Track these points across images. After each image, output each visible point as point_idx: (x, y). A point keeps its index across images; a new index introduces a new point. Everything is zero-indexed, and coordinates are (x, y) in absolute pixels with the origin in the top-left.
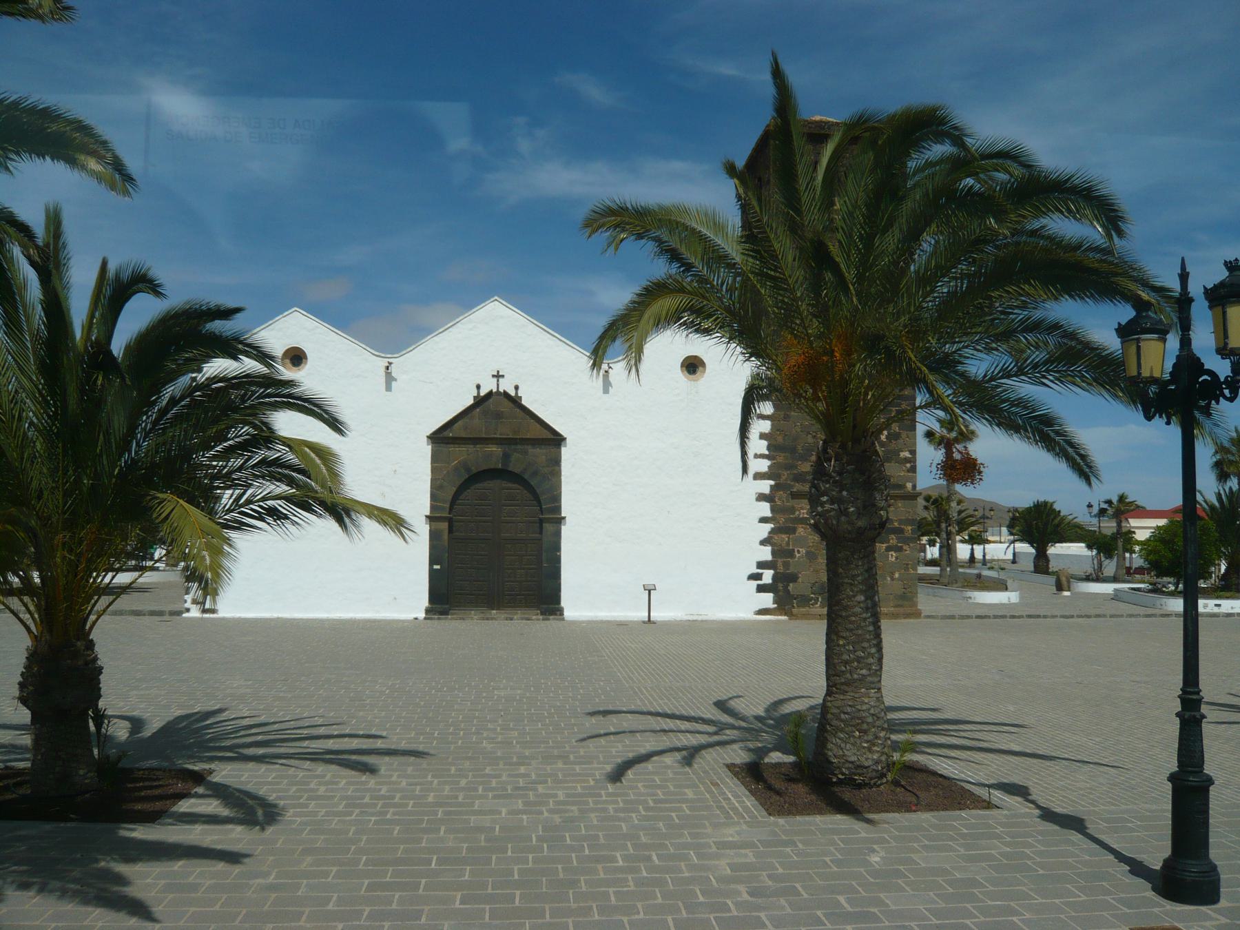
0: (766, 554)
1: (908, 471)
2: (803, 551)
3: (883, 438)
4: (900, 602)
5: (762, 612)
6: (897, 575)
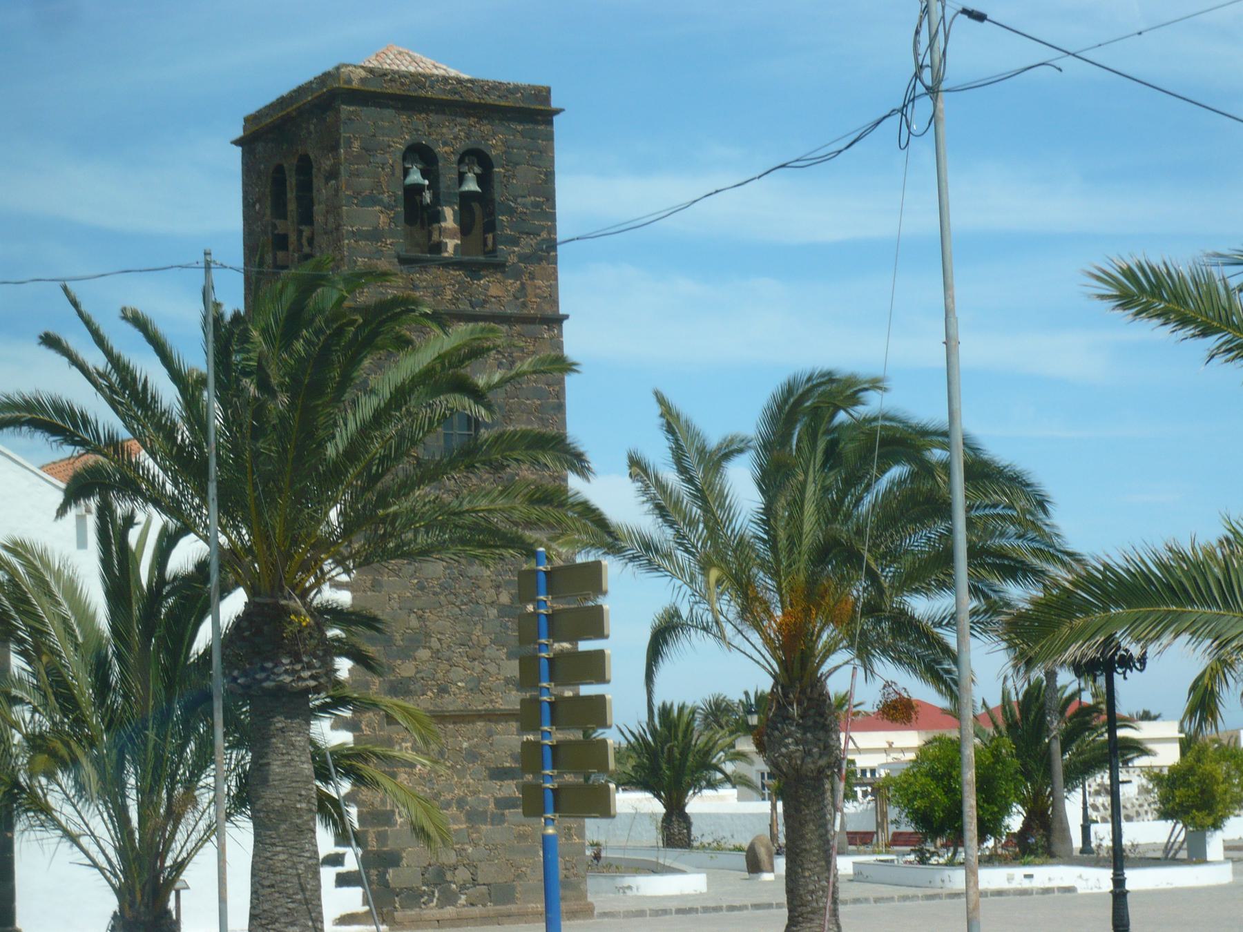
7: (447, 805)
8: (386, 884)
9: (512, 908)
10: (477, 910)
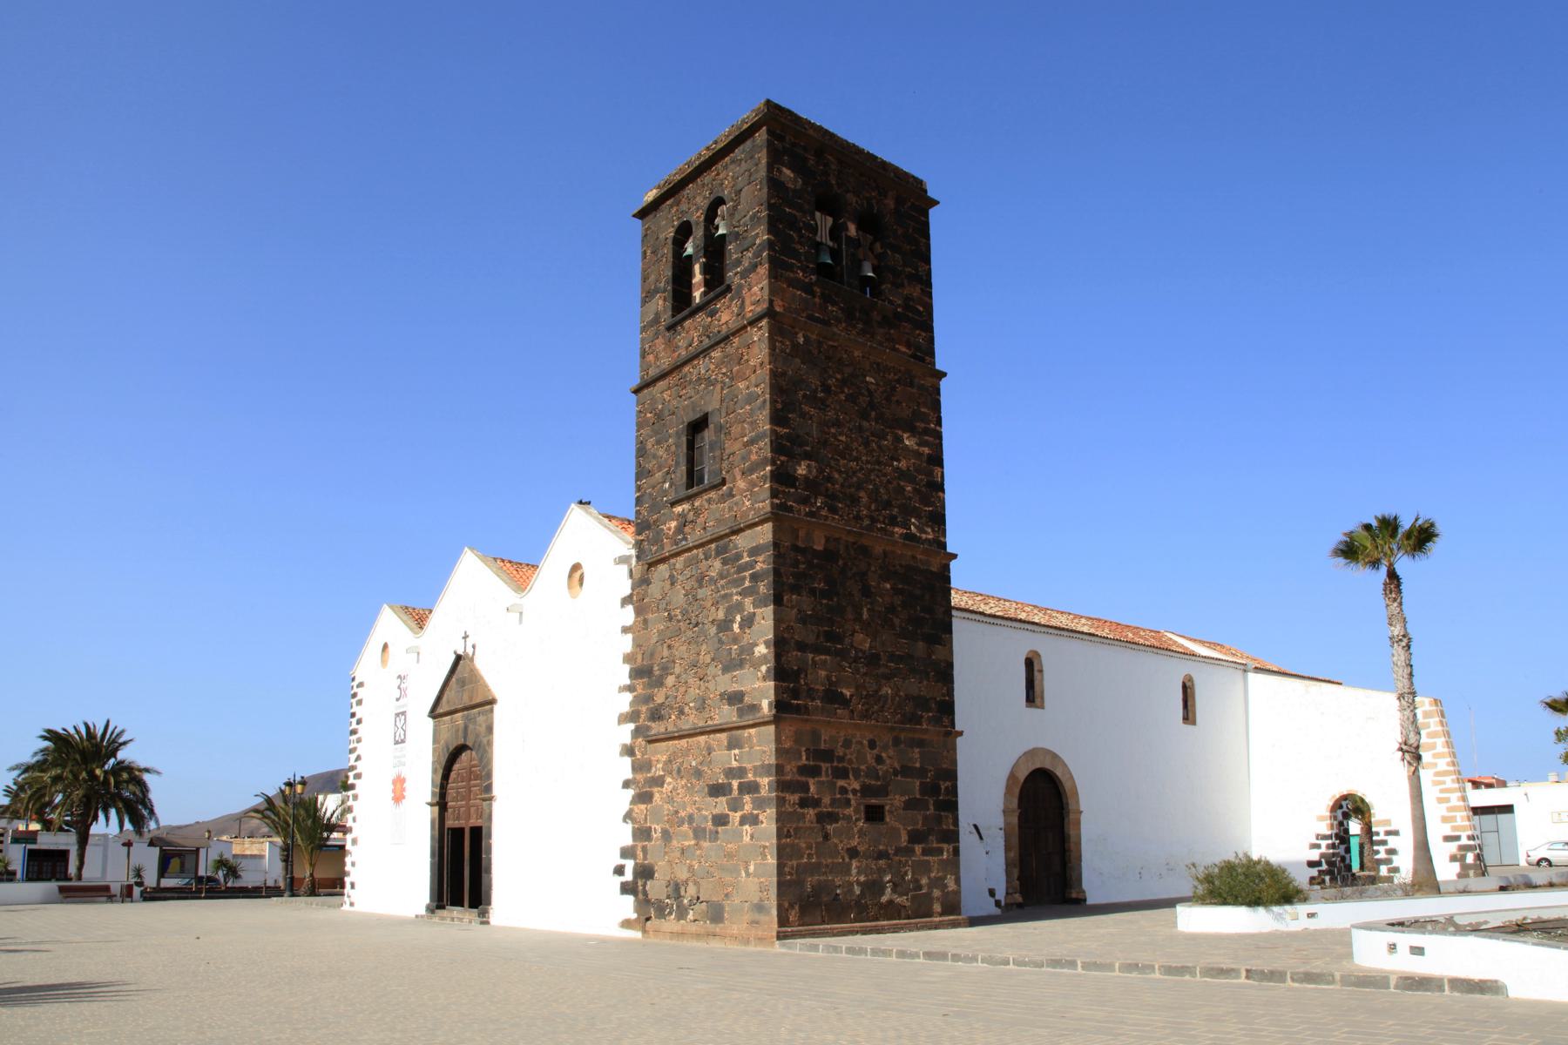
0: (625, 836)
1: (764, 678)
2: (659, 828)
3: (736, 627)
4: (757, 916)
5: (626, 924)
6: (752, 868)
7: (681, 823)
8: (645, 893)
9: (718, 928)
10: (693, 928)
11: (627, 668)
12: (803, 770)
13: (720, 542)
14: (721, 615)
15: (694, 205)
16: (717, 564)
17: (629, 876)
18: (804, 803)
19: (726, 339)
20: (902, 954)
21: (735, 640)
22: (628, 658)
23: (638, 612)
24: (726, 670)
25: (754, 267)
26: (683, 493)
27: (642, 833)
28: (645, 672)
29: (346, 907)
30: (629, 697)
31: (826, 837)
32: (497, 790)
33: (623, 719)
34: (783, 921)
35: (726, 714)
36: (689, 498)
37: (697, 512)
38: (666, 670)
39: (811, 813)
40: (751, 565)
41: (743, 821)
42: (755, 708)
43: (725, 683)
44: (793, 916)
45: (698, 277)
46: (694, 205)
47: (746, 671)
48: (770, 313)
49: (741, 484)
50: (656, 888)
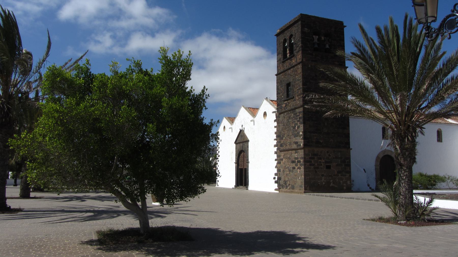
5: (276, 190)
10: (289, 190)
11: (275, 135)
12: (311, 158)
13: (293, 110)
14: (293, 125)
15: (287, 35)
16: (293, 115)
17: (276, 179)
18: (310, 165)
19: (294, 67)
20: (326, 196)
21: (296, 131)
22: (276, 133)
23: (278, 123)
24: (294, 137)
25: (299, 51)
26: (286, 99)
27: (279, 170)
28: (279, 136)
29: (217, 186)
30: (276, 141)
31: (316, 172)
32: (250, 160)
33: (275, 146)
34: (305, 189)
35: (294, 146)
36: (287, 100)
37: (289, 103)
38: (283, 136)
39: (312, 167)
40: (299, 115)
41: (298, 168)
42: (300, 145)
43: (294, 140)
44: (308, 189)
45: (288, 52)
46: (287, 35)
47: (298, 138)
48: (302, 62)
49: (297, 98)
50: (282, 182)
